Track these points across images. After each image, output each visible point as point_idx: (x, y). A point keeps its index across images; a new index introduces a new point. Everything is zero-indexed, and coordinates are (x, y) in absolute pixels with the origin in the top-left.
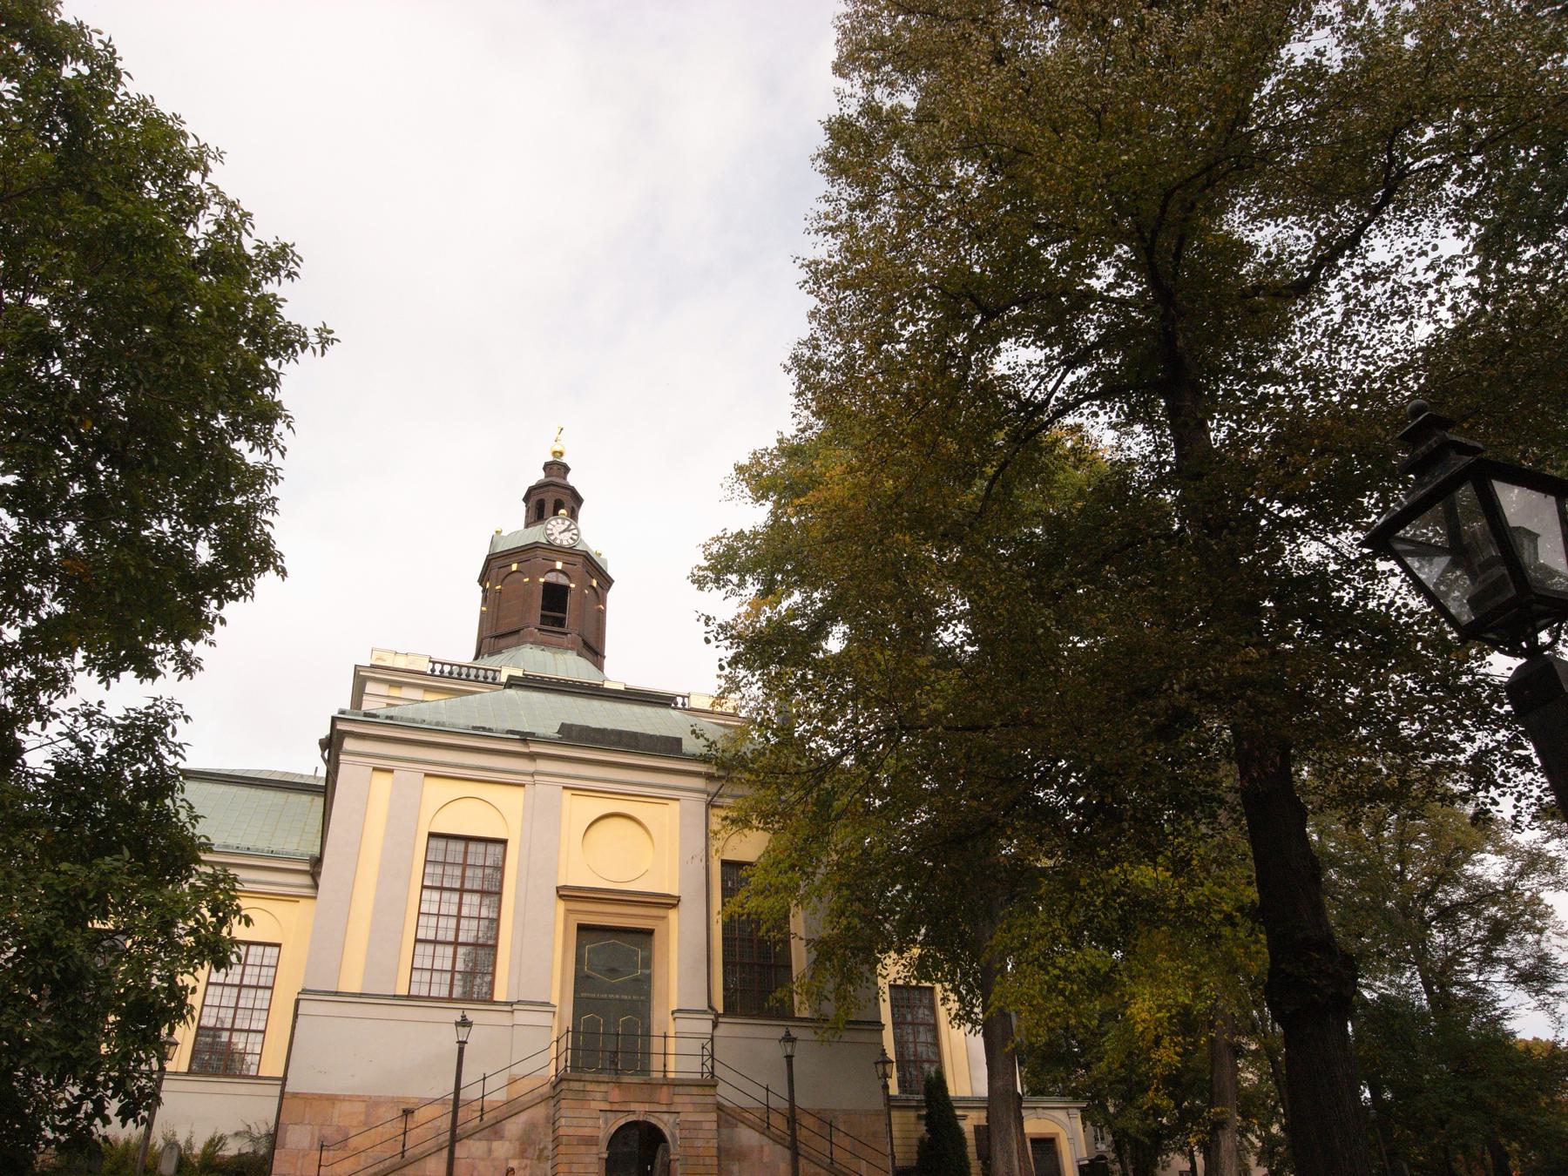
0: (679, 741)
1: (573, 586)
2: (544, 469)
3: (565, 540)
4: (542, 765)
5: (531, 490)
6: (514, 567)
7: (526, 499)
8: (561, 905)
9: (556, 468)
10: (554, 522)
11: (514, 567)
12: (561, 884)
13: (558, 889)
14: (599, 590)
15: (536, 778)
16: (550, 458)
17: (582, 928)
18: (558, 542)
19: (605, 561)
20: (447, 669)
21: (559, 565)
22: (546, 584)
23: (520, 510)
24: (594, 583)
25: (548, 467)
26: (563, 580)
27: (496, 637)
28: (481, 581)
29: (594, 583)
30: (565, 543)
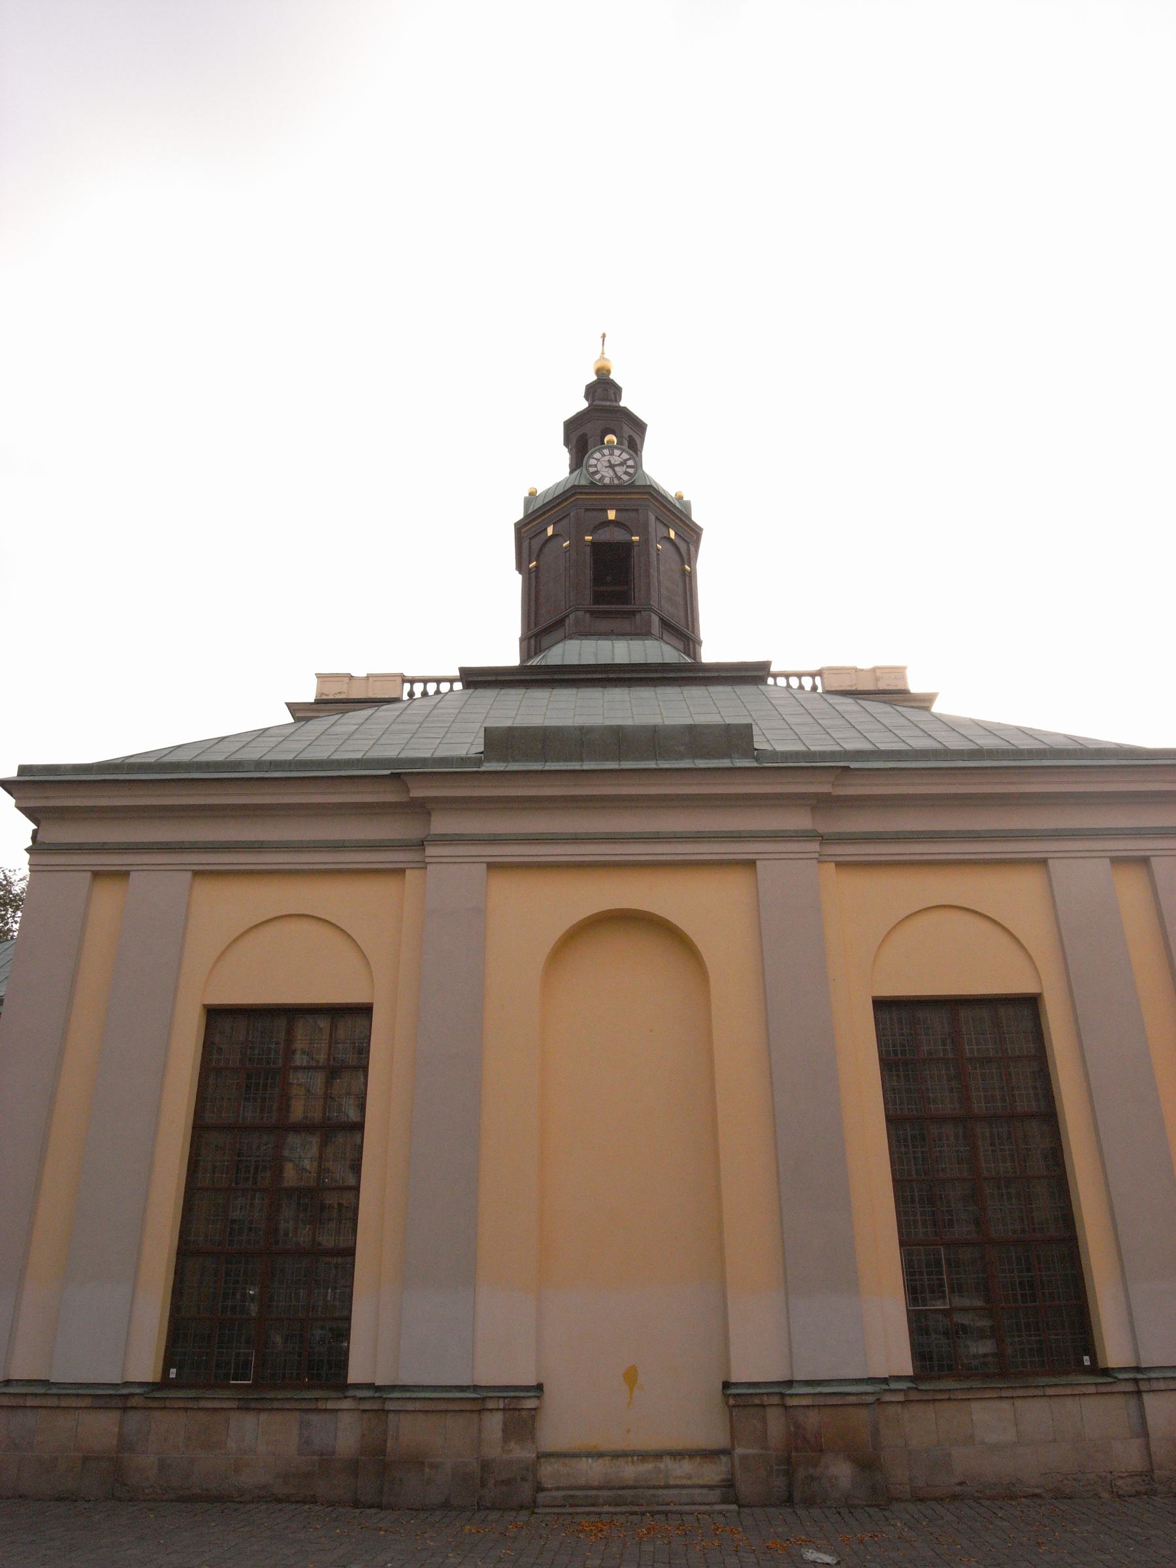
2: (587, 397)
4: (441, 824)
6: (550, 531)
7: (567, 442)
10: (597, 455)
11: (550, 531)
14: (682, 546)
15: (431, 851)
18: (607, 481)
19: (687, 505)
20: (431, 688)
21: (612, 515)
22: (593, 544)
24: (672, 534)
25: (591, 391)
26: (619, 535)
27: (536, 635)
28: (519, 567)
29: (672, 534)
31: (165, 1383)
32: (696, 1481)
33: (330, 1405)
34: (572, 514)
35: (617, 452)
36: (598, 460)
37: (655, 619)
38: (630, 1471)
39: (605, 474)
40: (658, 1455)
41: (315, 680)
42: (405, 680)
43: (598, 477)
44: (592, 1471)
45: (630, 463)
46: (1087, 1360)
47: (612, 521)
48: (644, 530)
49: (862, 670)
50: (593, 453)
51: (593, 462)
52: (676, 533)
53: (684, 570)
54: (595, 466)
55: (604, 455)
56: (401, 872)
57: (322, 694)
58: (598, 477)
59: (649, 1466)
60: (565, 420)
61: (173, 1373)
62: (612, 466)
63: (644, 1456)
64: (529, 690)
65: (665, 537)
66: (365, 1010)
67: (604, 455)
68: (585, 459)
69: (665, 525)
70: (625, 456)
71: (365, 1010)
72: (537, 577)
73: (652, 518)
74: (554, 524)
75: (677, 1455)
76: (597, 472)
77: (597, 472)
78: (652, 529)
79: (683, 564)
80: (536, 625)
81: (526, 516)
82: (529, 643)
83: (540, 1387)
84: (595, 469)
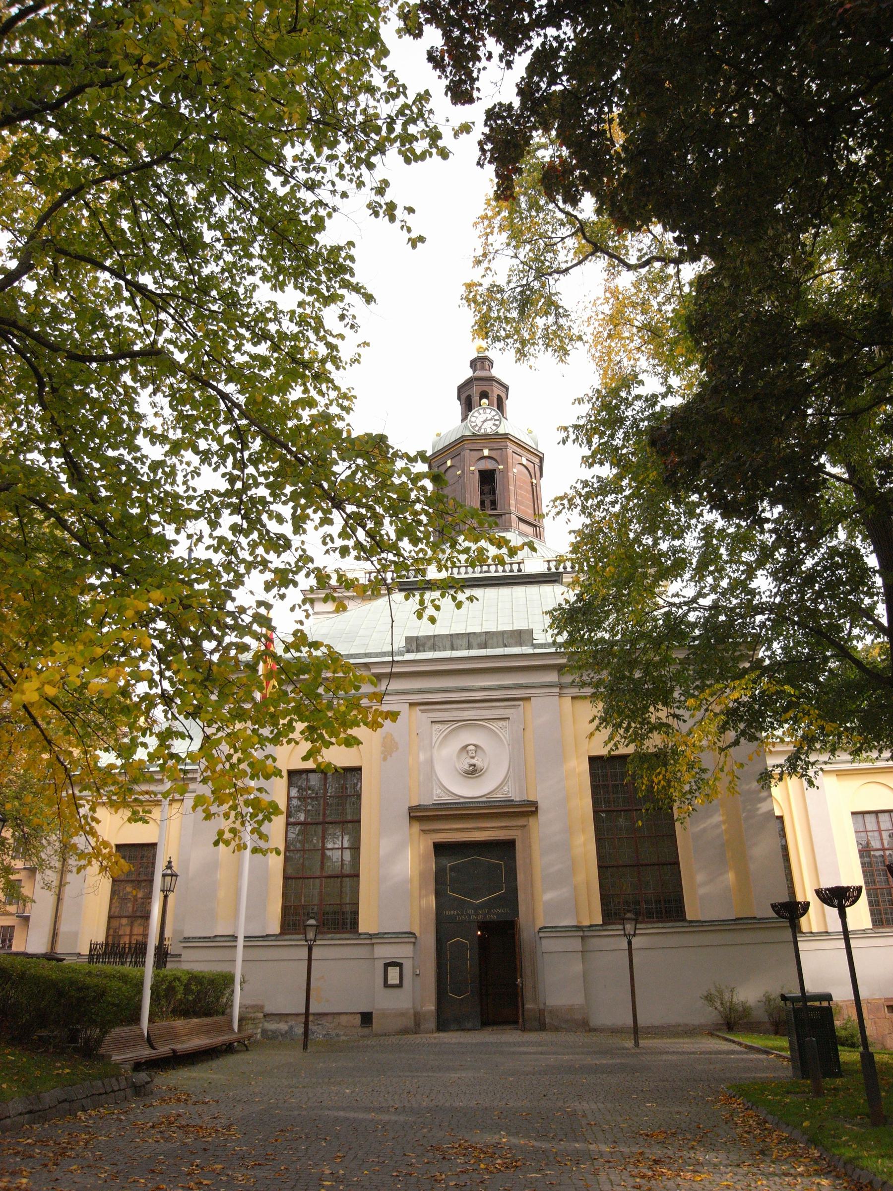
0: (531, 632)
1: (501, 467)
3: (488, 428)
5: (461, 389)
6: (449, 463)
7: (459, 398)
8: (417, 827)
11: (449, 463)
12: (415, 803)
13: (411, 809)
16: (474, 355)
17: (440, 849)
18: (482, 431)
23: (457, 407)
25: (473, 364)
30: (489, 431)
35: (488, 411)
45: (497, 417)
48: (505, 462)
51: (473, 419)
66: (358, 769)
70: (493, 413)
71: (358, 769)
73: (510, 451)
78: (510, 461)
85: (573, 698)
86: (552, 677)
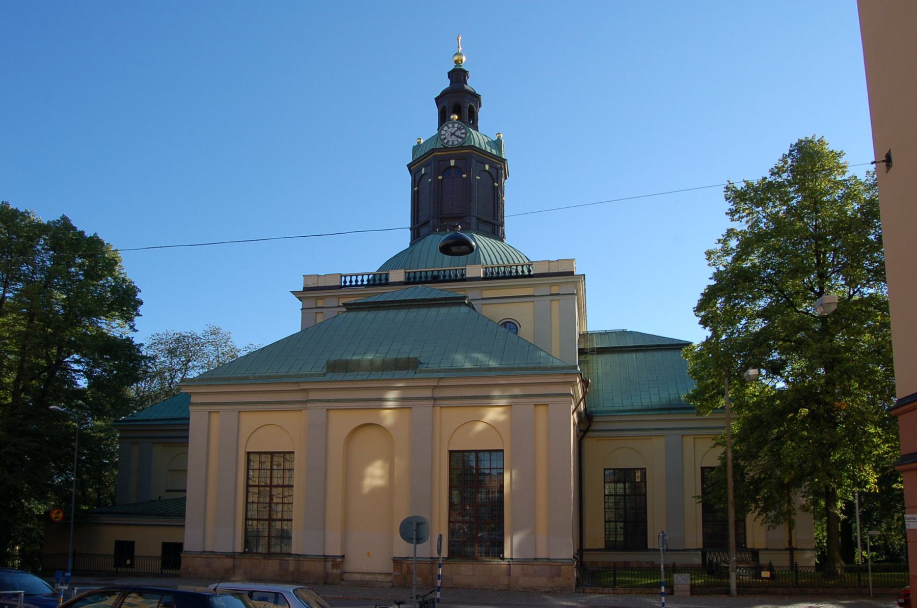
2: (449, 77)
9: (458, 75)
16: (452, 66)
29: (487, 167)
31: (245, 552)
32: (385, 581)
33: (287, 559)
34: (433, 164)
36: (446, 131)
37: (474, 219)
38: (367, 577)
39: (449, 139)
40: (375, 574)
41: (303, 278)
42: (341, 276)
43: (445, 141)
44: (357, 577)
46: (501, 555)
47: (452, 166)
49: (552, 261)
50: (443, 127)
52: (489, 166)
53: (494, 186)
54: (445, 135)
55: (449, 128)
56: (302, 410)
57: (306, 285)
58: (445, 141)
59: (373, 576)
60: (436, 97)
61: (247, 550)
62: (453, 134)
63: (371, 574)
64: (370, 312)
65: (483, 170)
67: (449, 128)
68: (443, 126)
69: (483, 163)
72: (418, 194)
74: (425, 167)
75: (380, 574)
76: (445, 138)
77: (445, 138)
79: (494, 182)
80: (417, 223)
81: (413, 161)
82: (414, 231)
83: (343, 556)
84: (444, 137)
85: (441, 407)
86: (428, 393)
